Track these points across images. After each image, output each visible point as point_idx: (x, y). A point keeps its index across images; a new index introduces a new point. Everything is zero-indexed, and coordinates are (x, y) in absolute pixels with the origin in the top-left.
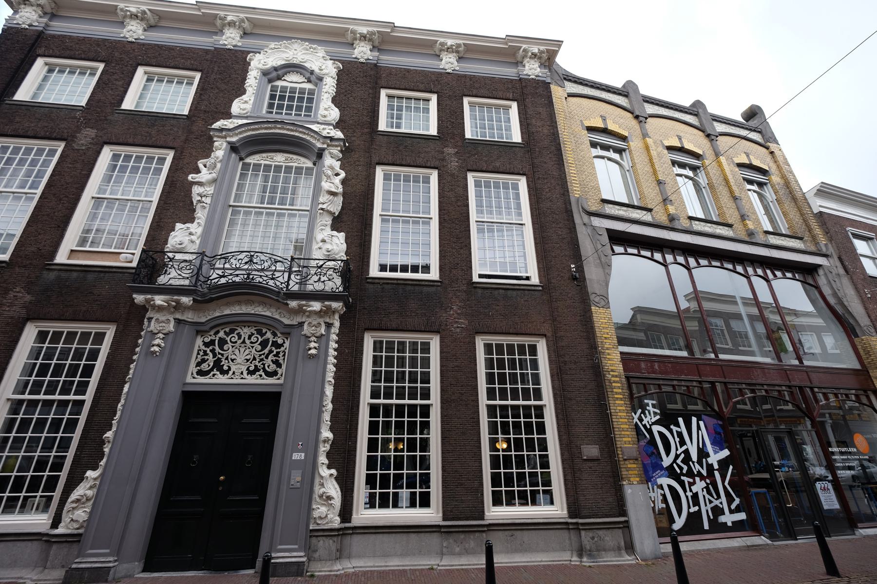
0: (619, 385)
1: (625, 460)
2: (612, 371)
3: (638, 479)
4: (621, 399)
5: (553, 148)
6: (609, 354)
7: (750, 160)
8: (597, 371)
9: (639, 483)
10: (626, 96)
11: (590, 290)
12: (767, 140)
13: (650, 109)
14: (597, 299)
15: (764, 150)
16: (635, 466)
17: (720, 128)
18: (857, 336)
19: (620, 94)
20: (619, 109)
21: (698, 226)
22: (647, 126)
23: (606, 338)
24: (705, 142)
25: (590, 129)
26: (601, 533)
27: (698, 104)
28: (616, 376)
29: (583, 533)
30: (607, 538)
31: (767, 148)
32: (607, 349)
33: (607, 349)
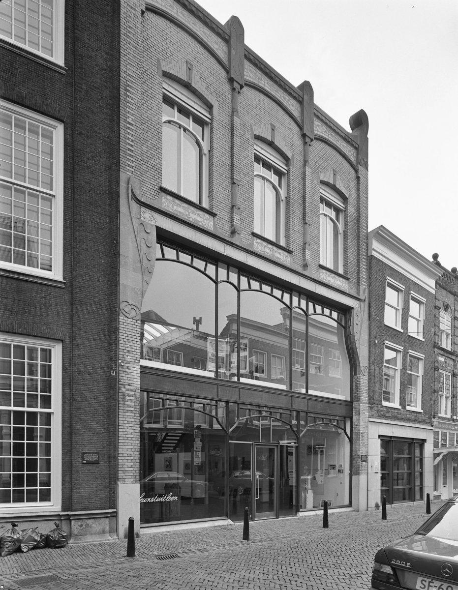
2: (129, 385)
8: (112, 385)
10: (227, 41)
11: (122, 297)
13: (251, 74)
14: (127, 309)
15: (353, 172)
17: (319, 129)
19: (218, 34)
20: (213, 60)
21: (259, 246)
22: (240, 98)
23: (129, 351)
25: (167, 75)
26: (90, 522)
28: (132, 390)
29: (73, 522)
31: (356, 171)
32: (128, 362)
33: (128, 362)
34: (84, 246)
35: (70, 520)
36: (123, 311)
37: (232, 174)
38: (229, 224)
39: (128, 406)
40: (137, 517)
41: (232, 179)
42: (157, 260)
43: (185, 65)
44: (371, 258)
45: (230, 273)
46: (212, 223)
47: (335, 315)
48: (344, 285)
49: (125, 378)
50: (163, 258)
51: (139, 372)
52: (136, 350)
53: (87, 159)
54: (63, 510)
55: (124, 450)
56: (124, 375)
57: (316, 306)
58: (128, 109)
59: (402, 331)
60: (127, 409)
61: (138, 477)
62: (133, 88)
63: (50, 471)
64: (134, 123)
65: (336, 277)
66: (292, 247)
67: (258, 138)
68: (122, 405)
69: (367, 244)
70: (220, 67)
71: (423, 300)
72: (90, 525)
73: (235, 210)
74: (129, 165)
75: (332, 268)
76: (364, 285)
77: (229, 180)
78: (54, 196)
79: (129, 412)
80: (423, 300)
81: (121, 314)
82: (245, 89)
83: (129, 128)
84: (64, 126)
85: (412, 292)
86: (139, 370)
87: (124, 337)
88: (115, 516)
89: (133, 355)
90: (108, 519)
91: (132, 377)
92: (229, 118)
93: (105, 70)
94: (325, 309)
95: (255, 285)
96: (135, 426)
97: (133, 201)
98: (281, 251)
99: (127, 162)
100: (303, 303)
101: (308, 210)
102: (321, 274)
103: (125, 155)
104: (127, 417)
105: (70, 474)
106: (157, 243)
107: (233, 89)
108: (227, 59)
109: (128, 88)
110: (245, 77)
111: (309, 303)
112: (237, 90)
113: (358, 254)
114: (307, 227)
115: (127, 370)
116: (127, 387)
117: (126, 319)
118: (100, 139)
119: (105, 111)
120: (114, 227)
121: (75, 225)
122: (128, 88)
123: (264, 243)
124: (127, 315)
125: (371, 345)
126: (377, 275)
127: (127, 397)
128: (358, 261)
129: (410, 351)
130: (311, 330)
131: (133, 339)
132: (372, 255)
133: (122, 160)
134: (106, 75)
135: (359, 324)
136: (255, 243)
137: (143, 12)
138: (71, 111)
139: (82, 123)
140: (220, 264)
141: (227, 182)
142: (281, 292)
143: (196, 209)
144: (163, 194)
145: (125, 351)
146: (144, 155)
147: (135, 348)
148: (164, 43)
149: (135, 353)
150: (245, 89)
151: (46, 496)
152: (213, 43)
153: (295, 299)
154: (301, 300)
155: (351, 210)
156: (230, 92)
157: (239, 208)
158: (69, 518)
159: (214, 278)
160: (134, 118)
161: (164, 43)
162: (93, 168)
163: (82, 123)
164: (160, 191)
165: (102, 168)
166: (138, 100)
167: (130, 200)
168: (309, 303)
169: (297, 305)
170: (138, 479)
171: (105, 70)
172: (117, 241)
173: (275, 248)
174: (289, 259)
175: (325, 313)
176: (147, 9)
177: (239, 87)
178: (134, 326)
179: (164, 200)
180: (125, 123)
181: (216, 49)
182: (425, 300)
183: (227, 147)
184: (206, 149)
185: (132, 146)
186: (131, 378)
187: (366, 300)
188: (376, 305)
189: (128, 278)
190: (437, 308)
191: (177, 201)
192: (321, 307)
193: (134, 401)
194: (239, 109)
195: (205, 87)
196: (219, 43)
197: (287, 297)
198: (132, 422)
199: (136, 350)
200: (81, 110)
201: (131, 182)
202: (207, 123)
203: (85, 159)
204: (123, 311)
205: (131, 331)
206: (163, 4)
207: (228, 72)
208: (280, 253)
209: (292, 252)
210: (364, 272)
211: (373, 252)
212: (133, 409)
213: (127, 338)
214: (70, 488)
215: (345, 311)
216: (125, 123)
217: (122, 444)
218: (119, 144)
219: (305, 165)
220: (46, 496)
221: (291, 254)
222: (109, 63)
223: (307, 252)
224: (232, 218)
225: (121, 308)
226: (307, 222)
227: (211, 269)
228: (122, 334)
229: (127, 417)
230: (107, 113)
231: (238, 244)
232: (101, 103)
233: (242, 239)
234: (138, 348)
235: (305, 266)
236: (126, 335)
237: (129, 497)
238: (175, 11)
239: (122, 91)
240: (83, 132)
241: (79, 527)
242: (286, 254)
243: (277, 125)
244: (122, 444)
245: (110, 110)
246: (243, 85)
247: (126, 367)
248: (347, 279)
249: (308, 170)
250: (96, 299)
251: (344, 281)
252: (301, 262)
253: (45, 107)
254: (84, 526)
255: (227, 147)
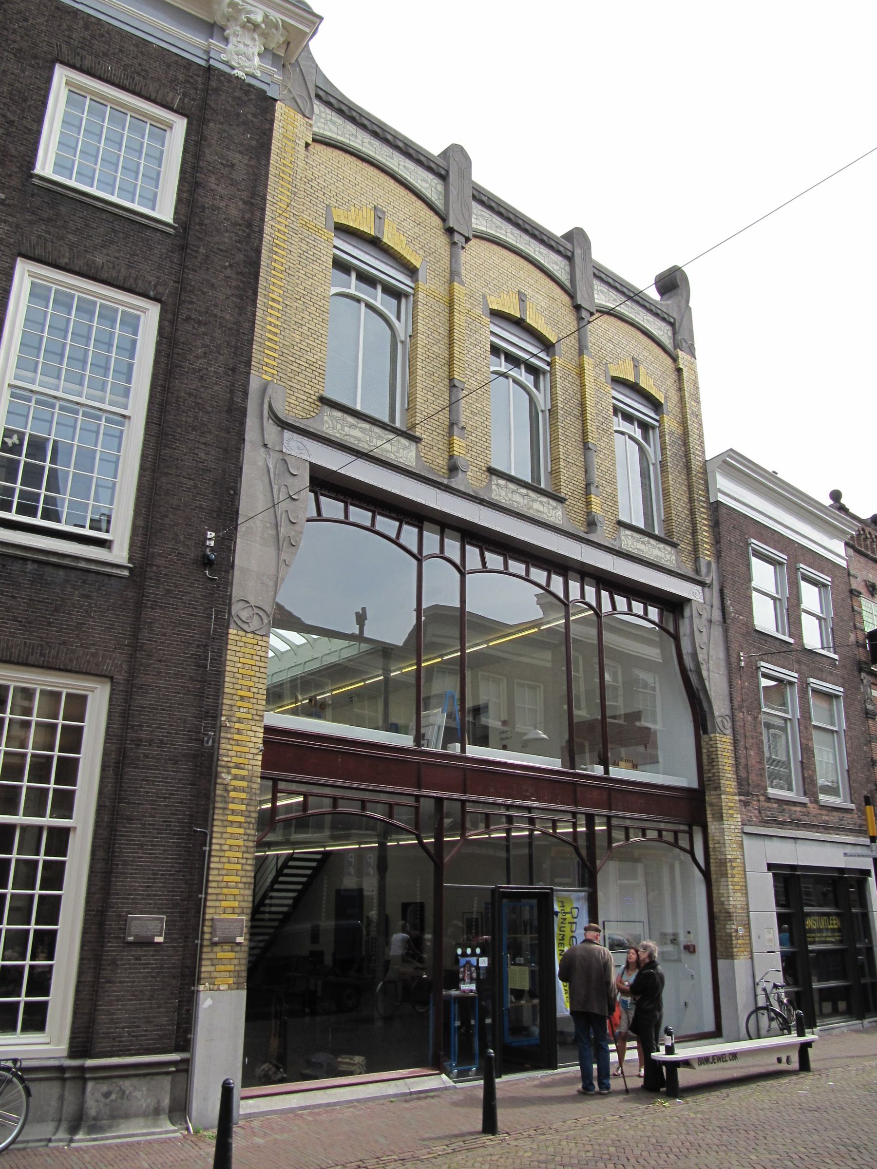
0: (244, 795)
1: (215, 944)
2: (238, 766)
3: (231, 981)
4: (240, 825)
5: (240, 257)
6: (239, 731)
7: (637, 375)
8: (204, 766)
9: (230, 988)
10: (443, 177)
11: (236, 592)
12: (678, 344)
13: (482, 221)
14: (244, 615)
15: (669, 361)
16: (231, 955)
17: (603, 297)
18: (706, 732)
19: (429, 169)
20: (419, 203)
21: (501, 492)
22: (464, 256)
23: (242, 698)
24: (569, 319)
25: (342, 230)
26: (127, 1084)
27: (577, 236)
28: (243, 778)
29: (90, 1085)
30: (137, 1094)
31: (675, 359)
34: (174, 502)
35: (85, 1080)
36: (236, 619)
37: (451, 371)
38: (446, 455)
39: (233, 812)
40: (236, 1080)
41: (451, 380)
42: (308, 521)
43: (372, 212)
44: (716, 507)
45: (446, 540)
46: (413, 454)
47: (653, 613)
48: (668, 557)
49: (230, 753)
50: (319, 518)
51: (260, 741)
52: (256, 696)
53: (196, 357)
54: (72, 1055)
55: (218, 910)
56: (229, 747)
57: (616, 597)
58: (273, 280)
59: (792, 641)
60: (230, 818)
61: (244, 974)
62: (284, 249)
63: (52, 959)
64: (281, 300)
65: (652, 542)
66: (564, 492)
67: (496, 314)
68: (220, 811)
69: (706, 481)
70: (431, 213)
71: (826, 579)
72: (127, 1092)
73: (456, 430)
74: (267, 365)
75: (641, 525)
76: (707, 555)
77: (446, 382)
78: (129, 418)
79: (235, 825)
80: (826, 579)
81: (232, 625)
82: (474, 241)
83: (272, 307)
84: (162, 308)
85: (802, 565)
86: (262, 735)
87: (235, 670)
88: (185, 1068)
89: (251, 706)
90: (169, 1078)
91: (247, 750)
92: (446, 286)
93: (240, 225)
94: (633, 602)
95: (494, 560)
96: (246, 855)
97: (270, 421)
98: (544, 499)
99: (265, 359)
100: (590, 592)
101: (591, 427)
102: (623, 538)
103: (261, 349)
104: (228, 836)
105: (95, 968)
106: (311, 491)
107: (454, 244)
108: (443, 202)
109: (275, 249)
110: (474, 226)
111: (603, 592)
112: (460, 244)
113: (691, 500)
114: (589, 453)
115: (236, 737)
116: (234, 771)
117: (241, 633)
118: (221, 326)
119: (234, 283)
120: (233, 467)
121: (162, 465)
122: (275, 249)
123: (512, 486)
124: (245, 627)
125: (732, 670)
126: (727, 538)
127: (232, 794)
128: (692, 512)
129: (812, 680)
130: (607, 636)
131: (253, 673)
132: (718, 502)
133: (256, 355)
134: (240, 233)
135: (704, 630)
136: (494, 487)
137: (307, 145)
138: (176, 285)
139: (191, 302)
140: (426, 524)
141: (442, 386)
142: (545, 574)
143: (384, 431)
144: (326, 408)
145: (235, 697)
146: (295, 348)
147: (255, 690)
148: (339, 184)
149: (255, 701)
150: (474, 241)
151: (36, 1019)
152: (419, 181)
153: (574, 586)
154: (586, 587)
155: (670, 423)
156: (448, 248)
157: (463, 428)
158: (81, 1075)
159: (415, 550)
160: (281, 292)
161: (339, 184)
162: (205, 372)
163: (191, 302)
164: (319, 404)
165: (221, 370)
166: (291, 265)
167: (265, 420)
168: (603, 592)
169: (578, 596)
170: (243, 980)
171: (240, 225)
172: (235, 491)
173: (532, 494)
174: (560, 513)
175: (635, 611)
176: (314, 140)
177: (463, 240)
178: (256, 647)
179: (326, 418)
180: (266, 301)
181: (426, 189)
182: (830, 579)
183: (442, 330)
184: (401, 335)
185: (275, 334)
186: (241, 752)
187: (715, 583)
188: (733, 591)
189: (251, 554)
190: (854, 594)
191: (351, 420)
192: (625, 599)
193: (246, 802)
194: (463, 272)
195: (405, 242)
196: (429, 181)
197: (557, 582)
198: (239, 846)
199: (256, 696)
200: (193, 283)
201: (269, 391)
202: (407, 295)
203: (191, 357)
204: (236, 619)
205: (250, 656)
206: (340, 132)
207: (444, 219)
208: (541, 502)
209: (566, 500)
210: (707, 531)
211: (719, 494)
212: (242, 819)
213: (241, 671)
214: (91, 1000)
215: (672, 606)
216: (266, 301)
217: (214, 897)
218: (254, 331)
219: (581, 353)
220: (36, 1019)
221: (562, 502)
222: (247, 216)
223: (593, 498)
224: (450, 445)
225: (233, 612)
226: (590, 446)
227: (409, 535)
228: (232, 664)
229: (228, 836)
230: (237, 287)
231: (462, 489)
232: (229, 272)
233: (471, 478)
234: (261, 691)
235: (591, 524)
236: (240, 665)
237: (221, 1013)
238: (359, 141)
239: (264, 253)
240: (193, 316)
241: (103, 1099)
242: (553, 503)
243: (528, 292)
244: (214, 897)
245: (242, 282)
246: (471, 237)
247: (236, 731)
248: (674, 545)
249: (588, 363)
250: (186, 598)
251: (669, 548)
252: (582, 518)
253: (132, 280)
254: (113, 1097)
255: (443, 331)
